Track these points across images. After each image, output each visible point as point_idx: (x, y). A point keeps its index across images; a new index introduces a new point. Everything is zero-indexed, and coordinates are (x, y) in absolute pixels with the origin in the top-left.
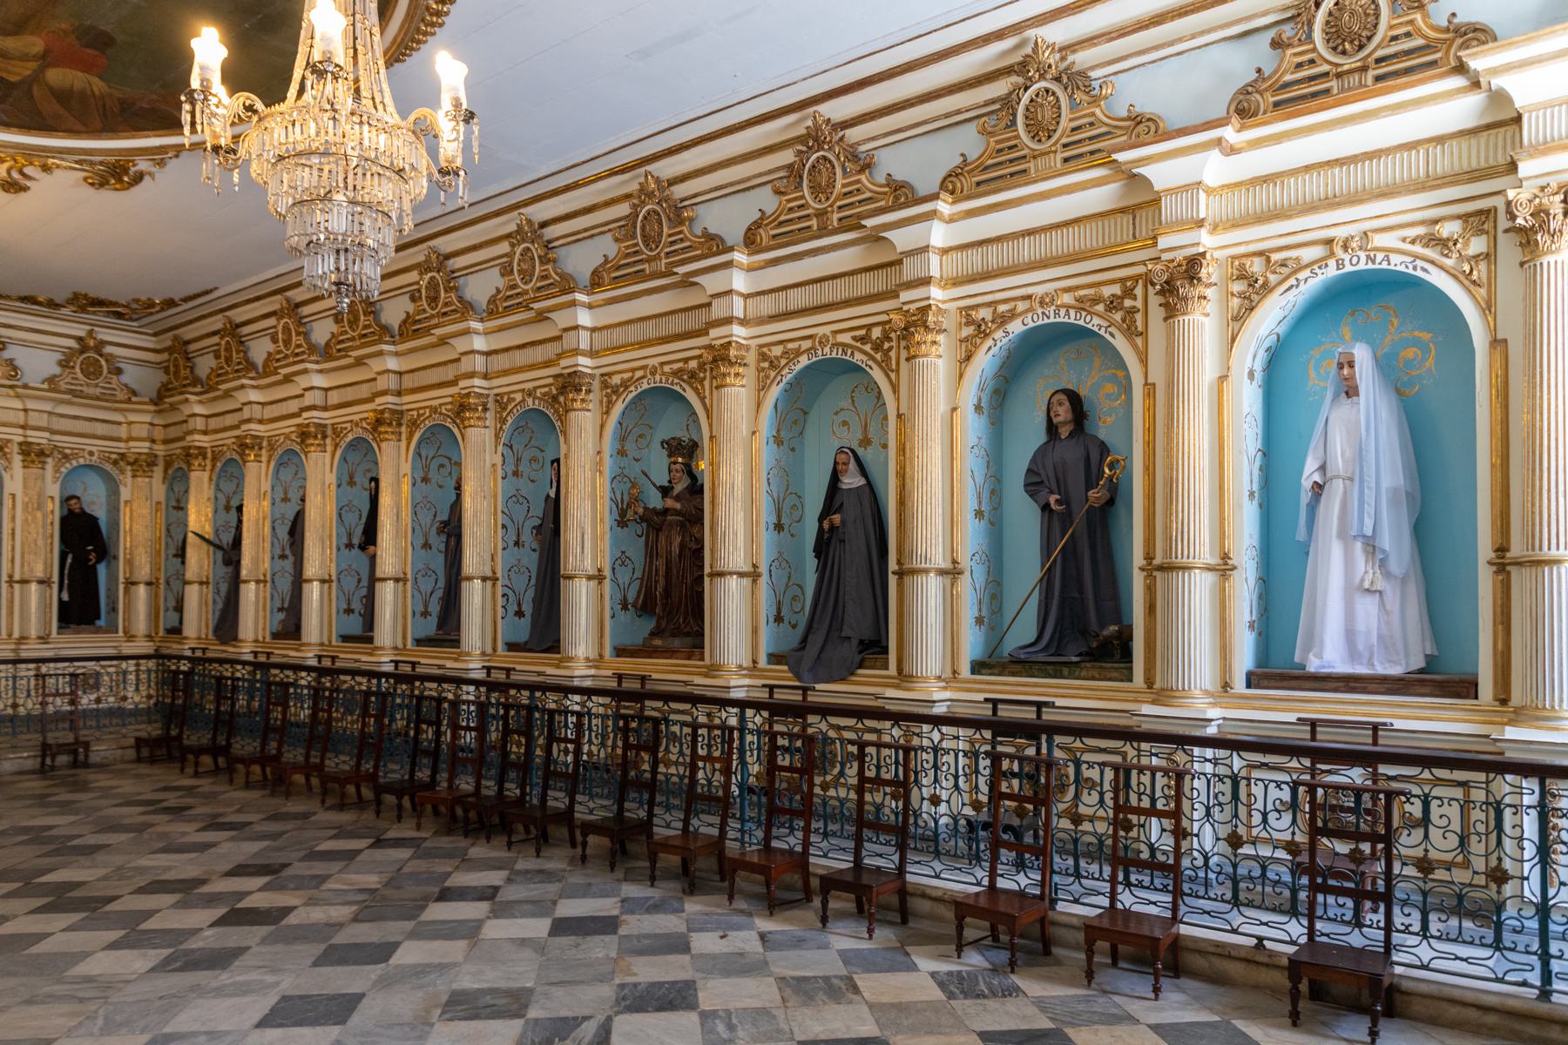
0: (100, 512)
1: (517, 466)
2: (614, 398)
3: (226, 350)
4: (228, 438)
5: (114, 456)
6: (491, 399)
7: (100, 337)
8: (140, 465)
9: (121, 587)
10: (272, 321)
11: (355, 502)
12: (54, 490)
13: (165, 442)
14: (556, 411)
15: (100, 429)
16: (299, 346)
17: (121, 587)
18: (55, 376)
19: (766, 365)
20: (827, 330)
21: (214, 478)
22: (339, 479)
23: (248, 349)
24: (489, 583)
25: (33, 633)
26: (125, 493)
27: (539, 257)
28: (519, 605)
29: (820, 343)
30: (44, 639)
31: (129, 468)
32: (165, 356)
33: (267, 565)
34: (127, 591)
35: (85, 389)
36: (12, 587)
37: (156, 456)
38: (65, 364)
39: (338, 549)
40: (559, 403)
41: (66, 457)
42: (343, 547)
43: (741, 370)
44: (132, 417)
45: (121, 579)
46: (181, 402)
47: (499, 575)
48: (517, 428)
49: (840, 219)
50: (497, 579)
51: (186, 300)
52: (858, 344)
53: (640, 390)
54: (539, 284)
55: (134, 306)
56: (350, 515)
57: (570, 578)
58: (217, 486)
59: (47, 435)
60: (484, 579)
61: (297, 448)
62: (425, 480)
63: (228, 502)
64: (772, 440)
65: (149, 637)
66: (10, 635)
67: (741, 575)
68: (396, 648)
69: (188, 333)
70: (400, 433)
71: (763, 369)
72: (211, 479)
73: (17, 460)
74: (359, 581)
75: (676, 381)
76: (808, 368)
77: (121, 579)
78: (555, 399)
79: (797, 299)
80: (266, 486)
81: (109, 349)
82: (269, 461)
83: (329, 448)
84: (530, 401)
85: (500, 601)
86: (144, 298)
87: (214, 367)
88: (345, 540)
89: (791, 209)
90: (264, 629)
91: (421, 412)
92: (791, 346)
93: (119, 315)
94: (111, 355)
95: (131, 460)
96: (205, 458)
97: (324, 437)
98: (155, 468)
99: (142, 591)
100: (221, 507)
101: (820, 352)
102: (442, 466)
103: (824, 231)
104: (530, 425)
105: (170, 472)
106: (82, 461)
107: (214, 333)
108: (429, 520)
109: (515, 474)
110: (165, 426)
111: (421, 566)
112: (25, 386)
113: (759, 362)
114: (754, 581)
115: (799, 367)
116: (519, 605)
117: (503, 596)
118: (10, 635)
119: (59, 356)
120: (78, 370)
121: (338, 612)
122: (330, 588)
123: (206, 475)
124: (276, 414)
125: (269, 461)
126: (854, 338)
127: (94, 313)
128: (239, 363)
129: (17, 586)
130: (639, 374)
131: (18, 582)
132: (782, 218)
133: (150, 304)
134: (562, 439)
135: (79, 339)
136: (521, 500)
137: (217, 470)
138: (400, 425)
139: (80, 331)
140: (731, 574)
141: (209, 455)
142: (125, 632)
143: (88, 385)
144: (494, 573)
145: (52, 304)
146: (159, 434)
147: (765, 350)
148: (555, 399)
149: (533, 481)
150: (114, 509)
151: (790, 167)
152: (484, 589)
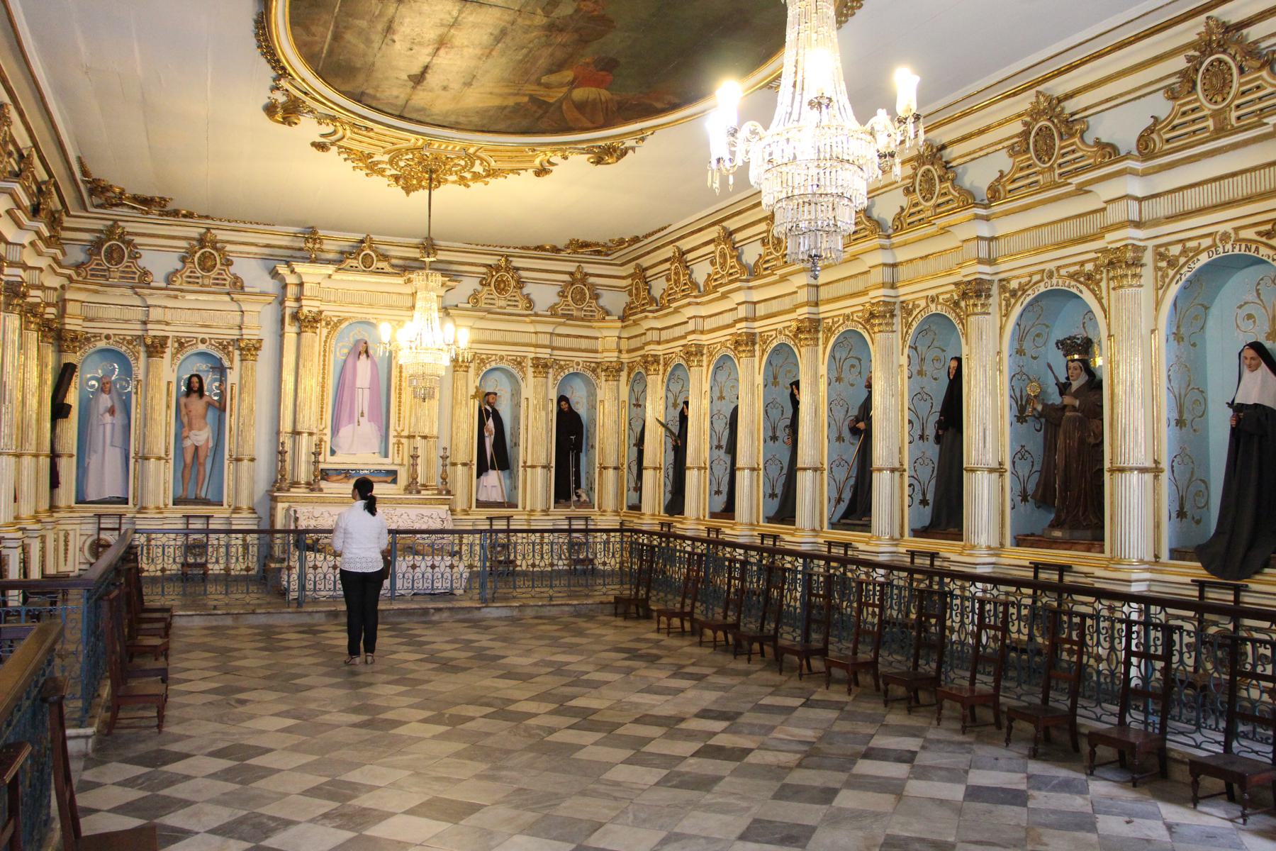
0: (582, 410)
1: (921, 367)
2: (1013, 301)
3: (675, 274)
4: (676, 347)
5: (593, 365)
6: (897, 306)
7: (585, 270)
8: (613, 371)
9: (597, 470)
10: (711, 248)
11: (778, 400)
12: (553, 395)
13: (629, 351)
14: (958, 315)
15: (584, 344)
16: (732, 267)
17: (597, 470)
18: (556, 304)
19: (1164, 264)
20: (1228, 227)
21: (665, 380)
22: (765, 380)
23: (692, 272)
24: (897, 474)
25: (539, 507)
26: (600, 394)
27: (939, 177)
28: (924, 494)
29: (1221, 240)
30: (546, 511)
31: (603, 373)
32: (629, 281)
33: (706, 454)
34: (601, 474)
35: (575, 313)
37: (622, 363)
38: (562, 294)
39: (765, 441)
40: (961, 308)
41: (561, 367)
42: (768, 439)
43: (1138, 270)
44: (605, 333)
45: (597, 465)
46: (641, 319)
47: (906, 466)
48: (921, 331)
49: (1239, 118)
50: (904, 470)
51: (646, 237)
52: (1264, 239)
53: (1037, 293)
54: (940, 201)
55: (610, 244)
56: (774, 411)
57: (973, 470)
58: (668, 386)
59: (549, 351)
60: (893, 470)
61: (731, 354)
62: (839, 379)
63: (676, 400)
64: (1171, 338)
65: (616, 512)
66: (524, 508)
67: (1142, 470)
68: (814, 530)
69: (646, 262)
70: (818, 339)
71: (1160, 269)
72: (663, 382)
73: (530, 371)
74: (782, 468)
75: (1073, 283)
76: (1207, 265)
77: (597, 465)
78: (956, 304)
79: (1193, 199)
80: (706, 386)
81: (592, 280)
82: (708, 366)
83: (757, 353)
84: (933, 306)
85: (907, 491)
86: (616, 238)
87: (666, 288)
88: (770, 434)
89: (1184, 114)
90: (704, 509)
91: (836, 319)
92: (1190, 244)
93: (598, 253)
94: (593, 285)
95: (604, 368)
96: (659, 364)
97: (754, 344)
98: (622, 373)
99: (610, 474)
100: (670, 404)
101: (1221, 250)
102: (853, 366)
103: (1221, 131)
104: (933, 328)
105: (632, 376)
106: (571, 370)
107: (666, 260)
108: (842, 416)
109: (920, 373)
110: (629, 338)
111: (835, 457)
112: (536, 315)
113: (1155, 261)
114: (1156, 477)
115: (1198, 265)
116: (924, 494)
117: (910, 486)
118: (524, 508)
119: (559, 289)
120: (569, 298)
121: (764, 497)
122: (758, 476)
123: (660, 377)
124: (714, 326)
125: (708, 366)
126: (1259, 233)
127: (582, 253)
128: (685, 284)
129: (529, 470)
130: (1036, 278)
131: (529, 467)
132: (1176, 122)
133: (621, 242)
134: (963, 341)
135: (571, 274)
136: (925, 397)
137: (668, 374)
138: (817, 331)
139: (571, 267)
140: (1131, 469)
141: (662, 362)
142: (600, 508)
143: (578, 309)
144: (902, 465)
145: (556, 250)
146: (624, 345)
147: (1162, 250)
148: (956, 304)
149: (935, 379)
150: (593, 407)
151: (1183, 74)
152: (892, 479)
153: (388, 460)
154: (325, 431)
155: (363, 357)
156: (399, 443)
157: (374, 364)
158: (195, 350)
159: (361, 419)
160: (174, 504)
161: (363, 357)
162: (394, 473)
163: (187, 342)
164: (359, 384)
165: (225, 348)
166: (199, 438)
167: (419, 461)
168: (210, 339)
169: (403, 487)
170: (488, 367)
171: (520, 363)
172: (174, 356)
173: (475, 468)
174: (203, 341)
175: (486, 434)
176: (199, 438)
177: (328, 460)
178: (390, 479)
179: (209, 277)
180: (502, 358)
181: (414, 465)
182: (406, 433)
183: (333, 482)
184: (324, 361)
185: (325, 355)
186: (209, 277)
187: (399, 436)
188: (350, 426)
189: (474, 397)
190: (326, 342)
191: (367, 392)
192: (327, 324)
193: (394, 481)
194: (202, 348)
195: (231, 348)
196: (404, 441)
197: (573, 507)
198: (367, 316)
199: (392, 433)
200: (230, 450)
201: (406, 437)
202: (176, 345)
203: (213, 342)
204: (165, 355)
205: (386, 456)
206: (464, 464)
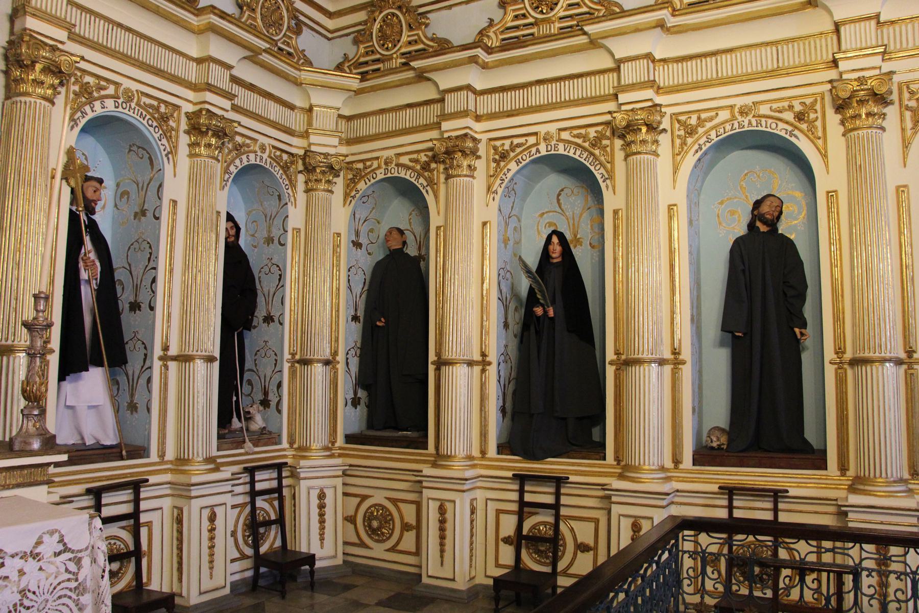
36: (166, 367)
45: (287, 356)
66: (162, 455)
73: (184, 140)
77: (287, 356)
118: (162, 455)
129: (172, 365)
131: (174, 358)
170: (98, 110)
171: (164, 119)
173: (54, 360)
175: (84, 275)
197: (248, 445)
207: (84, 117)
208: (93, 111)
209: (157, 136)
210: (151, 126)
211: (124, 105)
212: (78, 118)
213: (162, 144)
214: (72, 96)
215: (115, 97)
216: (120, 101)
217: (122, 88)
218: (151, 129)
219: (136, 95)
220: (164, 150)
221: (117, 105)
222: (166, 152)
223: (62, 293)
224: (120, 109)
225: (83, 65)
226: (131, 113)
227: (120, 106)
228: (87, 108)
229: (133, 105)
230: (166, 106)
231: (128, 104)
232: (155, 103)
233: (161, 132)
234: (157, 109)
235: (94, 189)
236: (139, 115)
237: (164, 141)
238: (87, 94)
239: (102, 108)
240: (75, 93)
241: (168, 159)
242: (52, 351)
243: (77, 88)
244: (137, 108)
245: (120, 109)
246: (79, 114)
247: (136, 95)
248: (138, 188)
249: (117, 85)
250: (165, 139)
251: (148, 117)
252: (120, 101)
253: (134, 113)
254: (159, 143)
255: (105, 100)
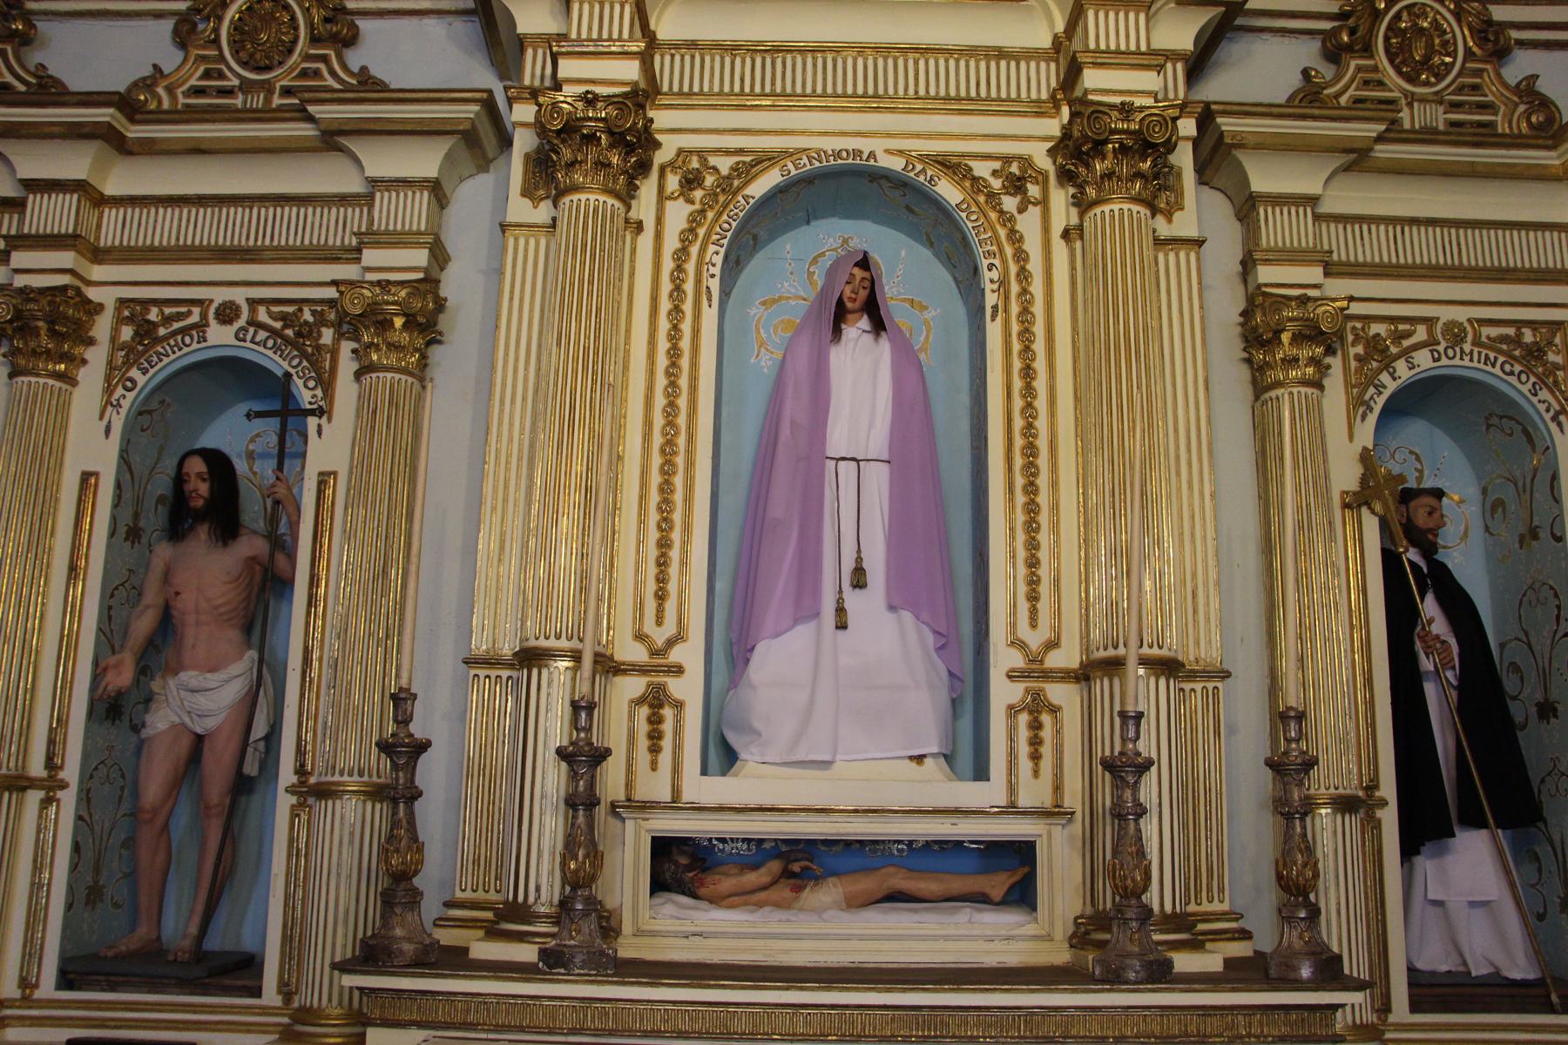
153: (992, 793)
154: (676, 655)
155: (857, 330)
156: (1037, 706)
157: (907, 363)
158: (193, 352)
159: (852, 599)
160: (67, 979)
161: (857, 330)
162: (1021, 854)
163: (168, 320)
164: (838, 440)
165: (307, 332)
166: (202, 701)
167: (1150, 789)
168: (253, 303)
169: (1062, 929)
170: (1403, 371)
171: (1535, 354)
172: (115, 376)
174: (227, 313)
175: (1427, 664)
176: (202, 701)
177: (688, 796)
178: (998, 884)
179: (267, 87)
180: (1455, 334)
181: (1127, 814)
182: (1067, 657)
183: (716, 901)
184: (675, 333)
185: (677, 310)
186: (267, 87)
187: (1034, 671)
188: (801, 636)
189: (1355, 502)
190: (681, 255)
191: (878, 479)
192: (691, 182)
193: (1023, 895)
194: (220, 336)
195: (327, 336)
196: (1062, 694)
198: (866, 145)
199: (1003, 658)
200: (300, 751)
201: (1067, 676)
202: (127, 333)
203: (262, 315)
204: (82, 374)
205: (981, 773)
206: (1345, 805)
207: (1380, 393)
208: (1394, 379)
209: (1525, 389)
210: (1512, 373)
211: (1451, 353)
212: (1372, 398)
213: (1540, 401)
214: (1353, 364)
215: (1430, 343)
216: (1441, 348)
217: (1440, 325)
218: (1513, 380)
219: (1469, 329)
220: (1548, 410)
221: (1436, 355)
222: (1552, 413)
223: (1390, 701)
224: (1444, 361)
225: (1356, 309)
226: (1466, 362)
227: (1443, 356)
228: (1384, 377)
229: (1467, 347)
230: (1534, 330)
231: (1458, 349)
232: (1511, 331)
233: (1533, 379)
234: (1516, 341)
235: (1428, 509)
236: (1483, 360)
237: (1544, 394)
238: (1378, 354)
239: (1410, 369)
240: (1358, 358)
241: (1560, 425)
242: (1383, 803)
243: (1360, 349)
244: (1476, 350)
245: (1444, 361)
246: (1372, 390)
247: (1469, 329)
248: (1517, 489)
249: (1429, 321)
250: (1545, 391)
251: (1501, 359)
252: (1441, 348)
253: (1471, 360)
254: (1534, 400)
255: (1413, 354)
